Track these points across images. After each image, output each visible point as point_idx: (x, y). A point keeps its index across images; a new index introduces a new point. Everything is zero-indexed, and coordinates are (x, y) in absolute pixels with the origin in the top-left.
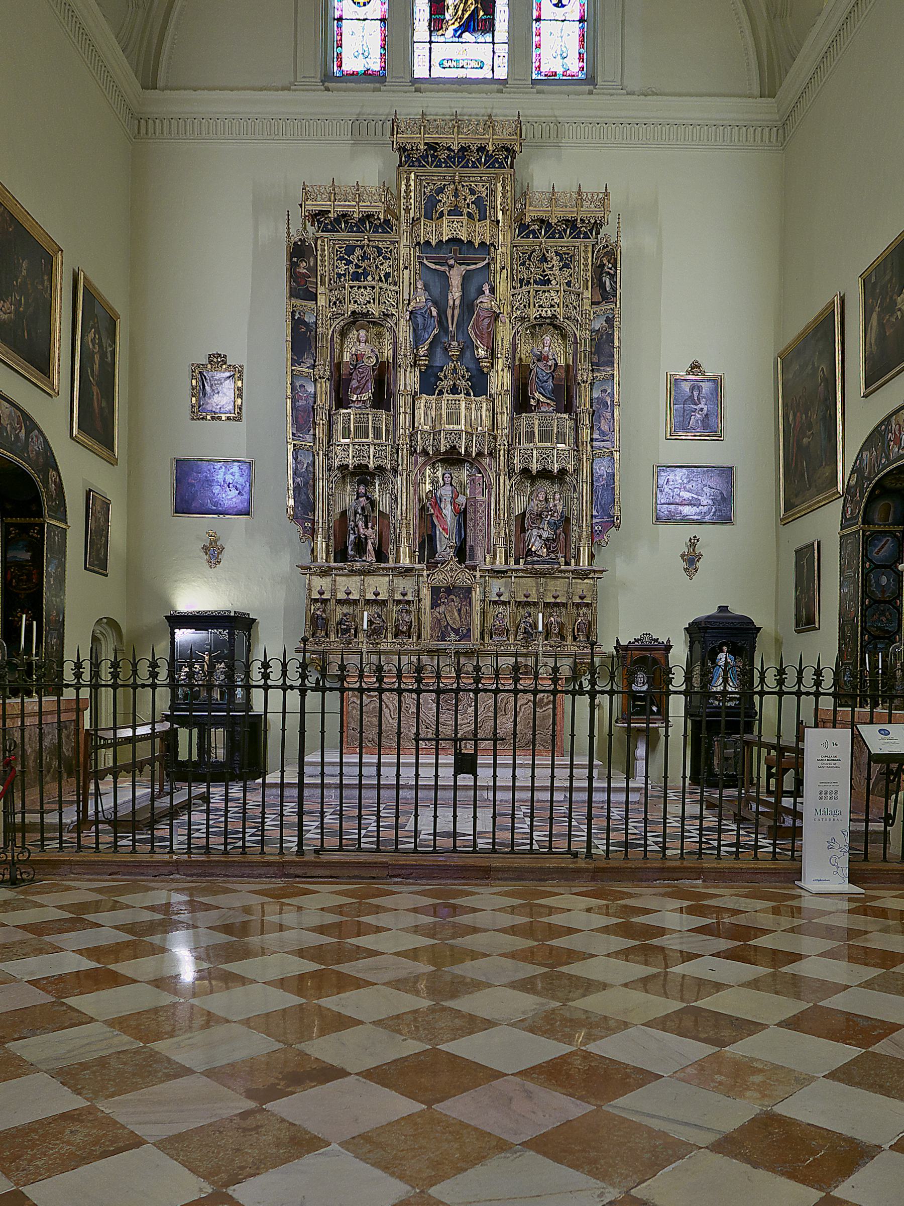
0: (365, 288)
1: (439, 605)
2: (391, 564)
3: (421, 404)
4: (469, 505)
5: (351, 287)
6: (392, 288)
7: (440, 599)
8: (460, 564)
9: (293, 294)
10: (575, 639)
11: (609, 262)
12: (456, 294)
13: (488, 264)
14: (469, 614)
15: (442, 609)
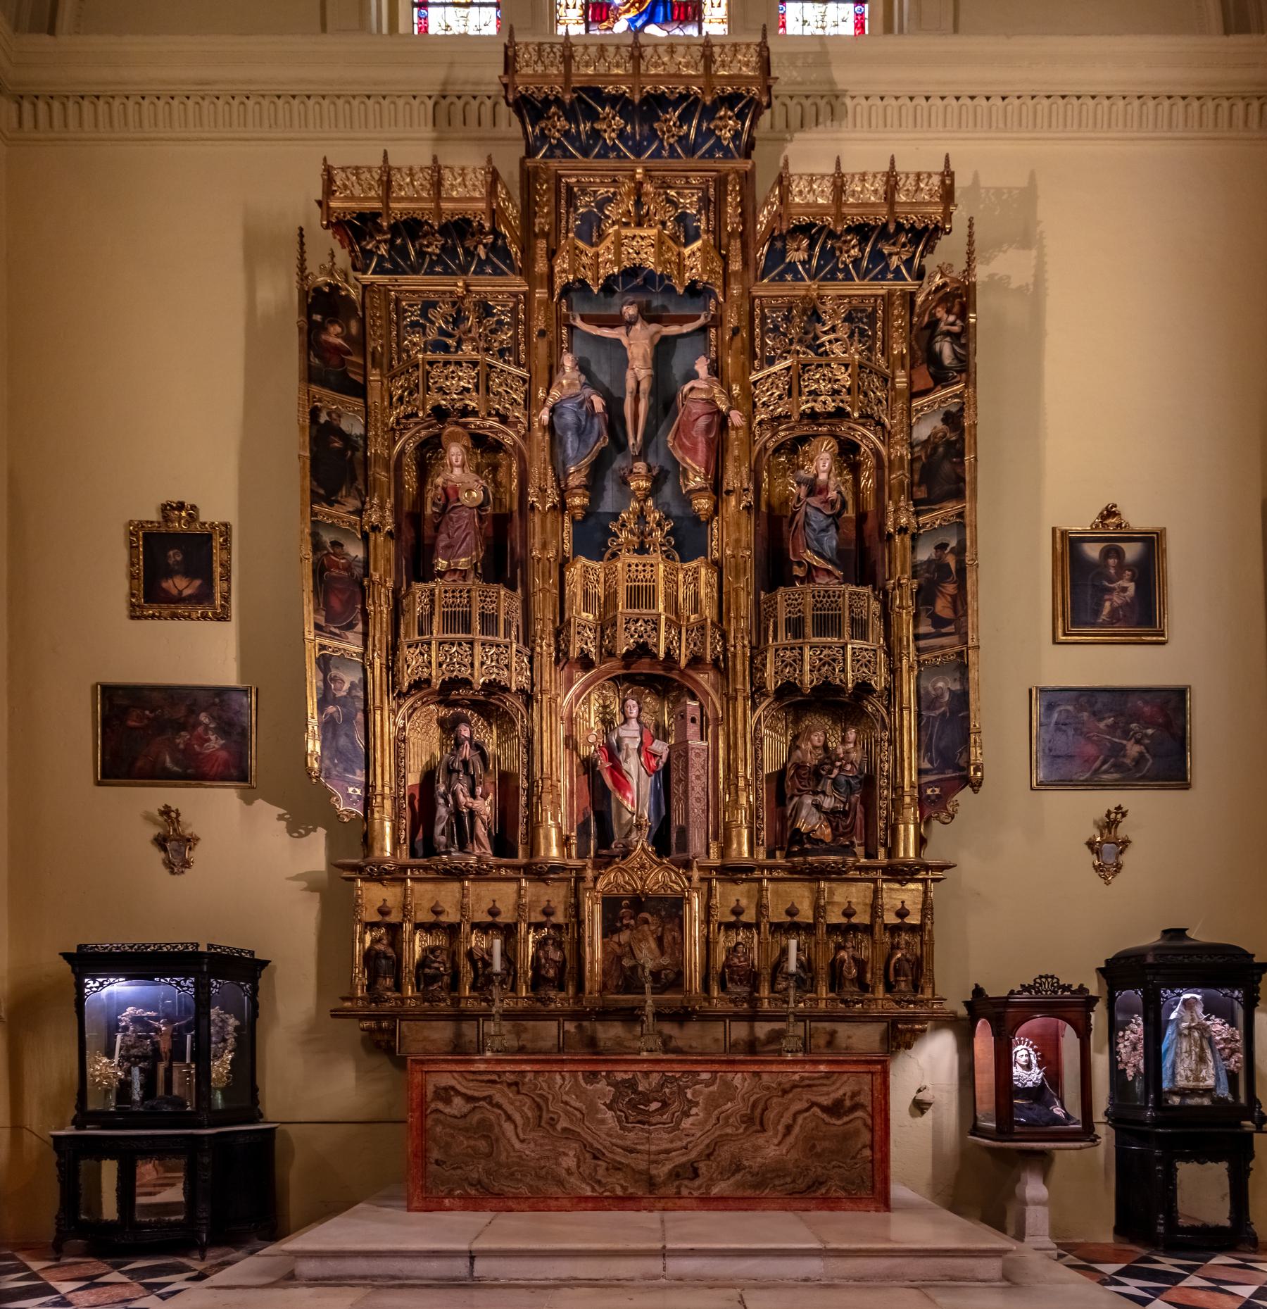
0: (459, 364)
1: (617, 931)
2: (521, 859)
3: (574, 574)
4: (674, 756)
5: (431, 363)
6: (515, 370)
7: (621, 919)
8: (659, 856)
9: (311, 376)
10: (889, 988)
11: (949, 312)
12: (639, 371)
13: (703, 329)
14: (679, 944)
15: (624, 937)
